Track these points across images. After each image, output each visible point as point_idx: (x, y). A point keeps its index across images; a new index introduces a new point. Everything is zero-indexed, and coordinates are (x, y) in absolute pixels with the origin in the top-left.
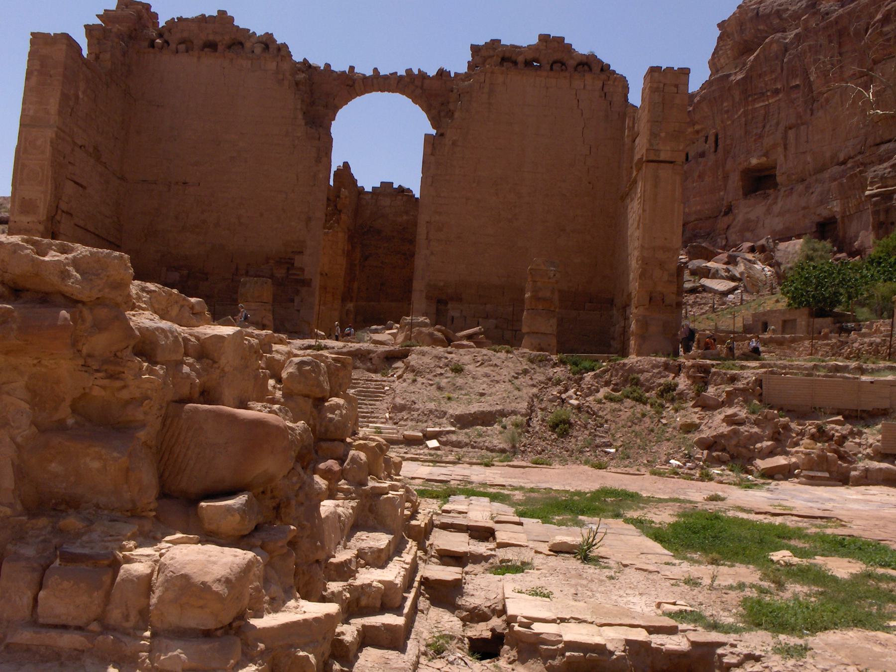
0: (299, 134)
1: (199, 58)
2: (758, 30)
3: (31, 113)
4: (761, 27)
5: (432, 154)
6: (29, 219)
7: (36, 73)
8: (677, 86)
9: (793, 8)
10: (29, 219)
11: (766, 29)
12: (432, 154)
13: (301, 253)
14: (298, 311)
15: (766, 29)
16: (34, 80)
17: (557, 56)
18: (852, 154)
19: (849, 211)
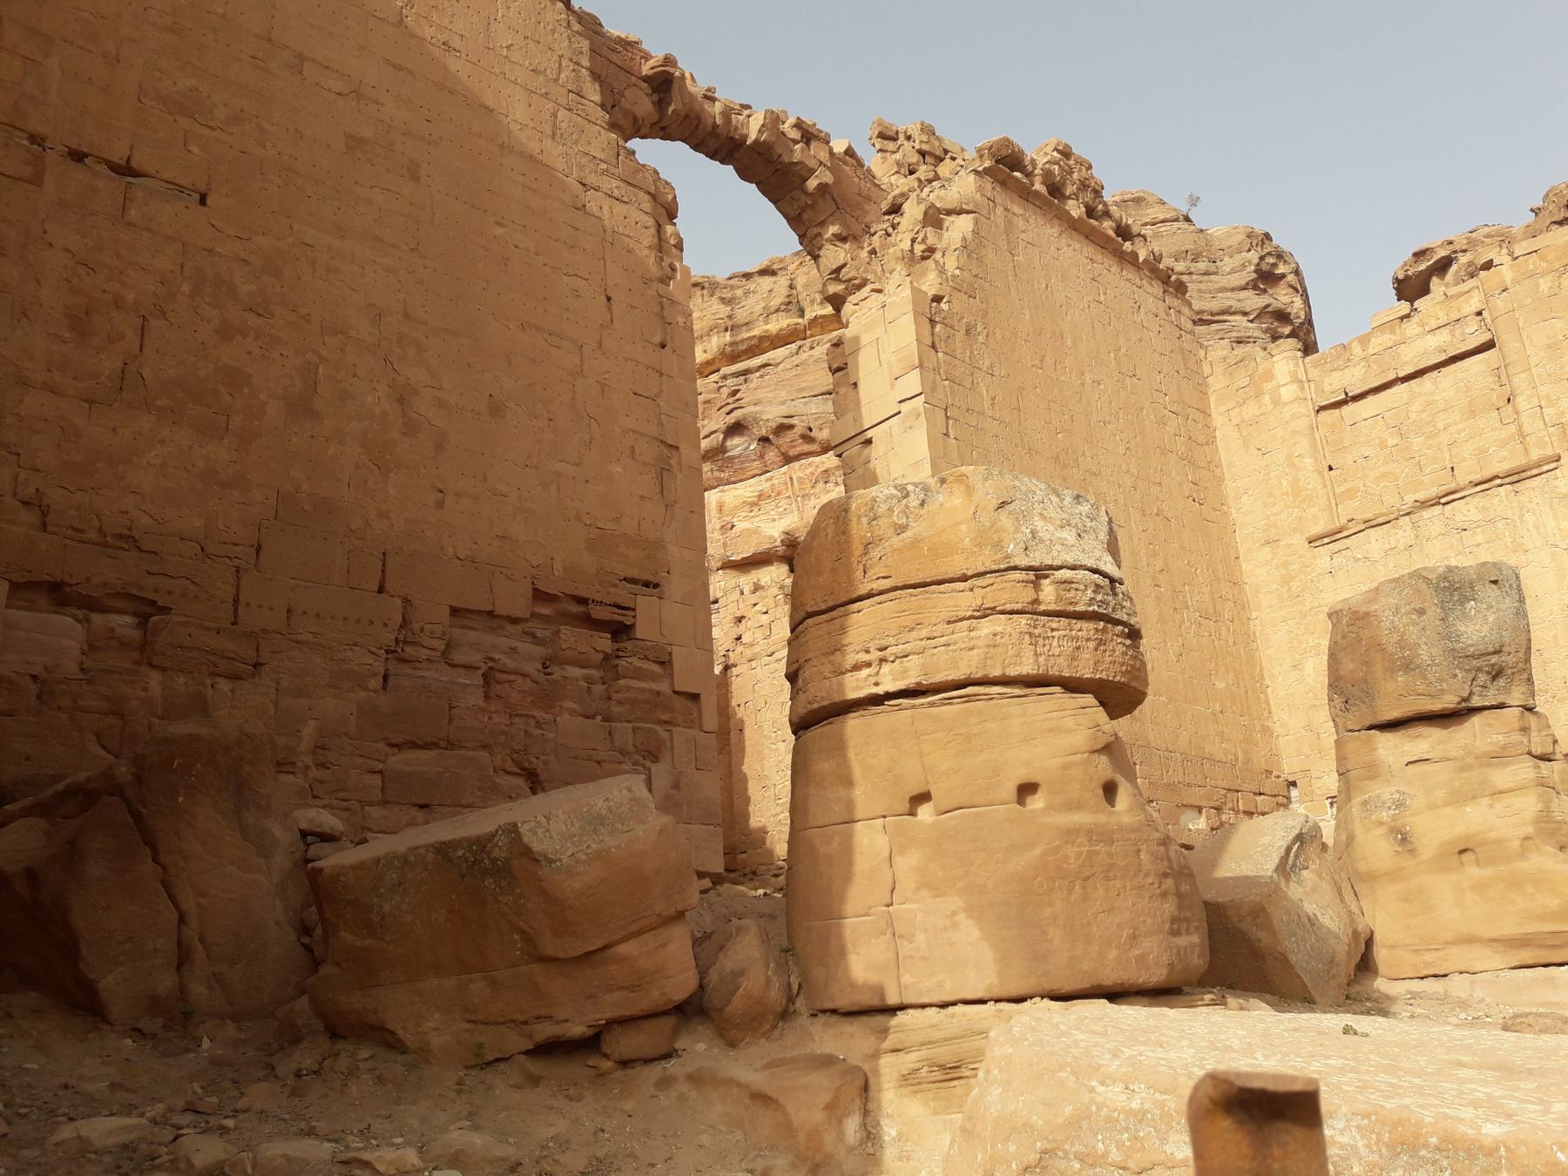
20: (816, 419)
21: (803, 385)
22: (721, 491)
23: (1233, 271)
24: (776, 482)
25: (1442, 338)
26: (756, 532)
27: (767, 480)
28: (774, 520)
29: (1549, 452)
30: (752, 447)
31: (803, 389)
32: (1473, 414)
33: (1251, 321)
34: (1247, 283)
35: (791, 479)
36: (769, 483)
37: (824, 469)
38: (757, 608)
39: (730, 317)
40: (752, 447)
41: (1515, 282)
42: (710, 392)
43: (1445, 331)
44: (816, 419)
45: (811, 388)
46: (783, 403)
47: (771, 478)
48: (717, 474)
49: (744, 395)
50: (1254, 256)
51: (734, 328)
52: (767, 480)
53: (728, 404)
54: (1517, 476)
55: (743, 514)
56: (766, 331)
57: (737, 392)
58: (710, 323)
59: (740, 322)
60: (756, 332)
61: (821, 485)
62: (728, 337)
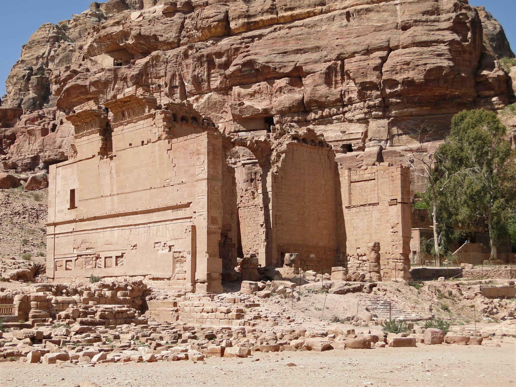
0: (225, 170)
1: (181, 125)
2: (139, 43)
3: (211, 173)
4: (142, 42)
5: (275, 182)
6: (215, 227)
7: (211, 153)
8: (407, 173)
9: (167, 36)
10: (215, 227)
11: (144, 43)
12: (275, 182)
13: (230, 230)
14: (230, 260)
15: (144, 43)
16: (211, 156)
17: (313, 138)
20: (279, 65)
21: (275, 48)
23: (445, 21)
24: (261, 87)
25: (369, 175)
27: (258, 86)
28: (259, 102)
29: (377, 202)
30: (253, 72)
31: (274, 50)
33: (446, 46)
34: (449, 28)
35: (267, 87)
36: (259, 87)
37: (280, 86)
38: (246, 195)
39: (247, 11)
40: (253, 72)
42: (238, 44)
44: (279, 65)
45: (278, 50)
46: (266, 56)
47: (259, 85)
48: (238, 80)
49: (251, 49)
50: (454, 15)
51: (249, 17)
52: (258, 86)
53: (244, 52)
54: (373, 204)
55: (248, 98)
56: (262, 20)
57: (248, 46)
58: (239, 13)
59: (251, 14)
60: (257, 19)
61: (278, 93)
62: (246, 20)
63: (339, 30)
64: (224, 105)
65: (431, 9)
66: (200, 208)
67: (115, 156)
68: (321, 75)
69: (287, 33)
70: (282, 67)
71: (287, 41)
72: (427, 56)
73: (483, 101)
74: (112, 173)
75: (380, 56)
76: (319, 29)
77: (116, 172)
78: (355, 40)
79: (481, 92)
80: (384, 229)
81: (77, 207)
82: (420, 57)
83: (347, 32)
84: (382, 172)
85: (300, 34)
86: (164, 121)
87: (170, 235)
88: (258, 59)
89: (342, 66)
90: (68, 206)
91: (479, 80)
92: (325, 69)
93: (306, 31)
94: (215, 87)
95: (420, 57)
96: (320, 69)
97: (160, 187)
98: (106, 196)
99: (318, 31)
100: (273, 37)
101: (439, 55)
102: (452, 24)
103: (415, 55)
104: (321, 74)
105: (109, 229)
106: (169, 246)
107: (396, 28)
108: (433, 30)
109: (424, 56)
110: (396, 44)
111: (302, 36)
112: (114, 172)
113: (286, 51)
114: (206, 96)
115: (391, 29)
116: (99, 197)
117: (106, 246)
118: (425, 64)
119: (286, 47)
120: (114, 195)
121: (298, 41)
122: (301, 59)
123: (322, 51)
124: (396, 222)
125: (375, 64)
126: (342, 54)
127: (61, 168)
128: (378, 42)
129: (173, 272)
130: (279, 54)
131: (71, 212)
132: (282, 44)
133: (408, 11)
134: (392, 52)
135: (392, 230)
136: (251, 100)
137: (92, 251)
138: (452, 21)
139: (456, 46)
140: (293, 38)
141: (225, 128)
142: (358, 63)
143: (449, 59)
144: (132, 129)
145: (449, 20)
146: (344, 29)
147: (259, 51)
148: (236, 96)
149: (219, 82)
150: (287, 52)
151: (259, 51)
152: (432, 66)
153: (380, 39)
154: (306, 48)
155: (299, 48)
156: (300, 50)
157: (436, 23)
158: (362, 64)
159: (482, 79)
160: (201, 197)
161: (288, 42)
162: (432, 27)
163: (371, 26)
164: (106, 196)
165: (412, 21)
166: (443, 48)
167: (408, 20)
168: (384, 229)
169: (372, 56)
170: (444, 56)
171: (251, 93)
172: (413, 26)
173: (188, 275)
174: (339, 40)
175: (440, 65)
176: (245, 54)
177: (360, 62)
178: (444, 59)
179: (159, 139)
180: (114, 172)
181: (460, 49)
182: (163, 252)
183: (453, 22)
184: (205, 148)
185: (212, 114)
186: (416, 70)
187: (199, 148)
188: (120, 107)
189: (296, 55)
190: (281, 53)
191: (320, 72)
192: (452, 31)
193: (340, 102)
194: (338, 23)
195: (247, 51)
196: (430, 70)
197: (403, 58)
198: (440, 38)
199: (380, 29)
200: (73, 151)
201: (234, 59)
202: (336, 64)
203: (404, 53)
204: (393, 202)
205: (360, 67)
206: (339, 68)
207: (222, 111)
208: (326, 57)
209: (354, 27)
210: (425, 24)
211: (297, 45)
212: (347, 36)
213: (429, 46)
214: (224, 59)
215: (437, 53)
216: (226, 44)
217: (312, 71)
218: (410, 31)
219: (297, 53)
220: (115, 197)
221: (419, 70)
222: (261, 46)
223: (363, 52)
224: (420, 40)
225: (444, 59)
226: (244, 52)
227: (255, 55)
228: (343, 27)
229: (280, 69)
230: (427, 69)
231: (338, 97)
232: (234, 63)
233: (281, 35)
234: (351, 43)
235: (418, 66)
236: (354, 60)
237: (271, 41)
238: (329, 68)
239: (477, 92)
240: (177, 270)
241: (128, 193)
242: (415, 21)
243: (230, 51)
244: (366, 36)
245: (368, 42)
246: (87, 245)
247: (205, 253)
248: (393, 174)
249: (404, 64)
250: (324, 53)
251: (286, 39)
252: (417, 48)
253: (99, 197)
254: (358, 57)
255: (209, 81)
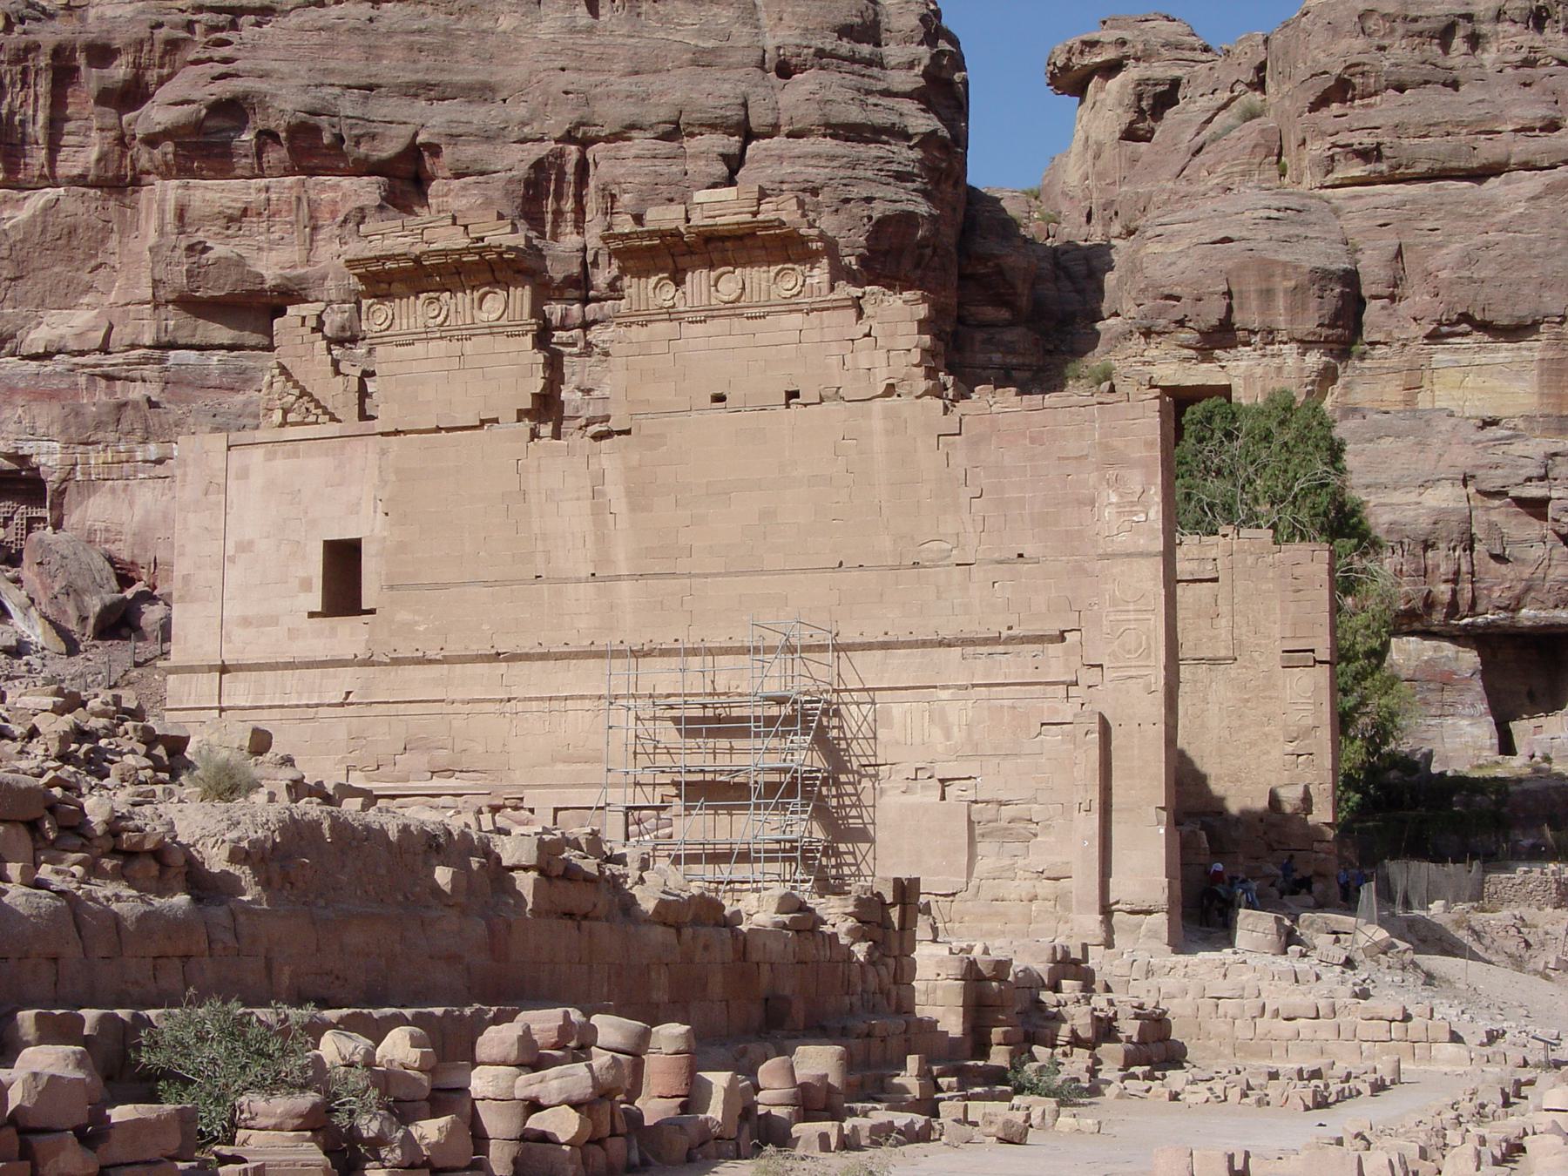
18: (73, 345)
19: (87, 473)
20: (351, 127)
21: (332, 64)
22: (186, 187)
26: (240, 262)
28: (260, 249)
29: (1231, 654)
32: (1199, 616)
33: (911, 148)
37: (358, 204)
41: (1237, 552)
42: (174, 26)
43: (1196, 563)
45: (344, 74)
53: (210, 60)
54: (1214, 661)
63: (568, 40)
64: (103, 241)
65: (859, 20)
66: (1129, 652)
67: (628, 432)
68: (511, 187)
69: (371, 20)
70: (362, 136)
71: (376, 47)
72: (869, 174)
73: (979, 336)
74: (603, 494)
75: (721, 150)
76: (486, 25)
77: (629, 493)
78: (626, 84)
79: (973, 309)
80: (1252, 744)
81: (372, 612)
82: (849, 173)
83: (596, 50)
84: (1250, 560)
85: (421, 31)
86: (920, 333)
87: (948, 737)
88: (274, 96)
89: (583, 168)
90: (315, 601)
91: (969, 270)
92: (525, 166)
93: (442, 23)
94: (76, 172)
95: (849, 173)
96: (506, 163)
97: (892, 568)
98: (566, 581)
99: (483, 31)
100: (321, 24)
101: (901, 177)
102: (922, 82)
103: (835, 164)
104: (510, 181)
105: (587, 704)
106: (942, 781)
107: (761, 65)
108: (869, 92)
109: (860, 172)
110: (770, 119)
111: (427, 39)
112: (615, 492)
113: (373, 81)
114: (38, 199)
115: (745, 65)
116: (522, 582)
117: (560, 766)
118: (869, 200)
119: (373, 69)
120: (618, 578)
121: (415, 54)
122: (432, 120)
123: (504, 101)
124: (1310, 722)
125: (710, 175)
126: (584, 124)
127: (259, 452)
128: (711, 102)
129: (970, 874)
130: (349, 87)
131: (333, 629)
132: (355, 53)
133: (794, 14)
134: (754, 143)
135: (1289, 748)
136: (228, 237)
137: (467, 783)
138: (919, 70)
139: (936, 154)
140: (397, 39)
141: (111, 327)
142: (649, 162)
143: (926, 194)
144: (731, 341)
145: (911, 65)
146: (581, 40)
147: (276, 65)
148: (170, 216)
149: (93, 153)
150: (379, 86)
151: (276, 65)
152: (890, 209)
153: (717, 94)
154: (451, 84)
155: (420, 77)
156: (429, 86)
157: (875, 71)
158: (661, 166)
159: (981, 270)
160: (1132, 616)
161: (381, 52)
162: (866, 80)
163: (676, 46)
164: (566, 581)
165: (812, 50)
166: (906, 155)
167: (797, 46)
168: (1252, 744)
169: (691, 145)
170: (914, 181)
171: (230, 211)
172: (812, 67)
173: (1085, 882)
174: (569, 75)
175: (911, 208)
176: (222, 68)
177: (657, 162)
178: (914, 190)
179: (890, 390)
180: (615, 492)
181: (944, 165)
182: (908, 799)
183: (925, 75)
184: (1149, 445)
185: (56, 269)
186: (842, 216)
187: (1117, 443)
188: (673, 255)
189: (406, 101)
190: (359, 88)
191: (510, 174)
192: (920, 102)
193: (577, 288)
194: (559, 15)
195: (226, 61)
196: (883, 222)
197: (797, 169)
198: (895, 119)
199: (708, 59)
200: (297, 392)
201: (161, 81)
202: (561, 155)
203: (797, 152)
204: (1295, 657)
205: (659, 180)
206: (570, 169)
207: (93, 263)
208: (524, 124)
209: (620, 40)
210: (846, 66)
211: (411, 66)
212: (597, 66)
213: (867, 141)
214: (120, 71)
215: (894, 167)
216: (131, 20)
217: (478, 167)
218: (805, 83)
219: (416, 96)
220: (625, 586)
221: (852, 217)
222: (275, 48)
223: (661, 128)
224: (842, 119)
225: (914, 190)
226: (210, 60)
227: (261, 77)
228: (579, 32)
229: (357, 144)
230: (876, 215)
231: (576, 269)
232: (165, 93)
233: (351, 23)
234: (617, 91)
235: (847, 201)
236: (634, 151)
237: (316, 39)
238: (539, 165)
239: (960, 305)
240: (982, 866)
241: (706, 576)
242: (820, 53)
243: (146, 48)
244: (664, 76)
245: (677, 96)
246: (442, 757)
247: (1153, 811)
248: (1298, 571)
249: (804, 190)
250: (521, 111)
251: (372, 40)
252: (835, 142)
253: (522, 582)
254: (640, 143)
255: (54, 147)
